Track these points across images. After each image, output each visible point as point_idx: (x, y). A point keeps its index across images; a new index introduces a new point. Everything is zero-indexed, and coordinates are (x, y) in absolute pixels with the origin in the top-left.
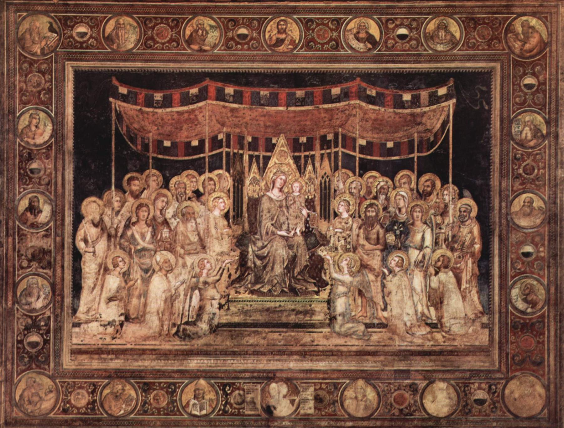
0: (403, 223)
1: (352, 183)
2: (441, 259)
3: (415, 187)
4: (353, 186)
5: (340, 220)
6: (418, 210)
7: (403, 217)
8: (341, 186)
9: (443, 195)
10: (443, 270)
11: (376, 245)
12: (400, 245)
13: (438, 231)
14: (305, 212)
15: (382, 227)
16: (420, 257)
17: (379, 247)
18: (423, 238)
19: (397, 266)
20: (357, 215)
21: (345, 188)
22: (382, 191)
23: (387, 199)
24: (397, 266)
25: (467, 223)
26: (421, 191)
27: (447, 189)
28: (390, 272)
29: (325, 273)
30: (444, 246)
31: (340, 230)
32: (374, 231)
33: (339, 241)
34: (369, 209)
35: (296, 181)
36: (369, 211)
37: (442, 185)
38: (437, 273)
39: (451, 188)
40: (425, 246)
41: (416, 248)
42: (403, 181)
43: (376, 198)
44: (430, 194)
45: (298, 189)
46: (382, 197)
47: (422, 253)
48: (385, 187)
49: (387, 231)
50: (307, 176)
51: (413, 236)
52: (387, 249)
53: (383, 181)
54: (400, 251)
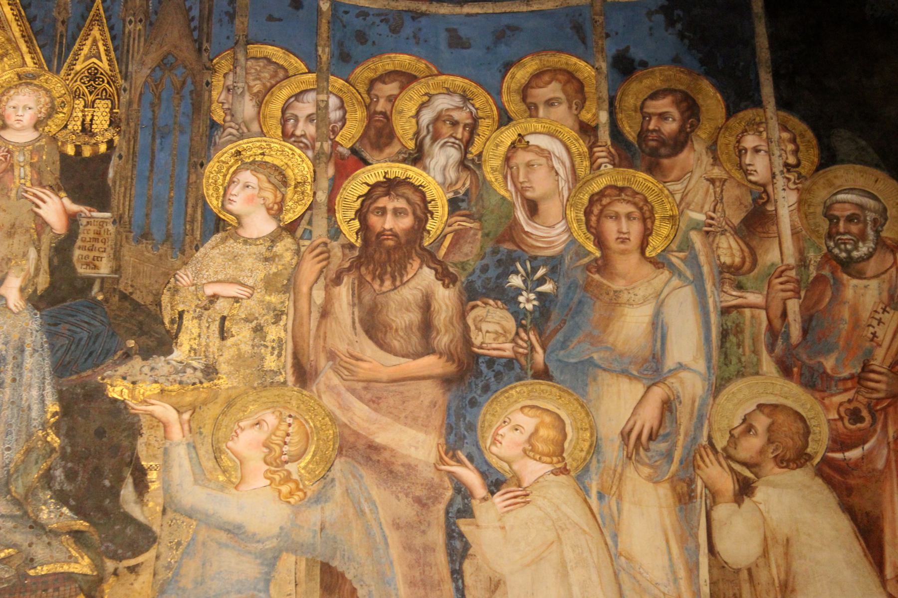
0: (555, 265)
1: (298, 96)
2: (761, 422)
3: (604, 117)
4: (306, 108)
5: (232, 246)
6: (623, 208)
7: (550, 233)
8: (247, 108)
9: (741, 152)
10: (775, 473)
11: (417, 356)
12: (539, 356)
13: (732, 298)
14: (54, 209)
15: (445, 276)
16: (649, 416)
17: (431, 364)
18: (658, 328)
19: (530, 450)
20: (320, 228)
21: (259, 115)
22: (446, 129)
23: (468, 164)
24: (530, 450)
25: (872, 267)
26: (630, 132)
27: (754, 126)
28: (495, 484)
29: (141, 486)
30: (768, 365)
31: (233, 290)
32: (410, 293)
33: (223, 334)
34: (383, 202)
35: (24, 79)
36: (383, 211)
37: (731, 111)
38: (745, 489)
39: (773, 124)
40: (670, 363)
41: (625, 373)
42: (542, 93)
43: (417, 157)
44: (679, 143)
45: (28, 118)
46: (443, 157)
47: (658, 393)
48: (456, 115)
49: (471, 295)
50: (78, 67)
51: (607, 322)
52: (472, 378)
53: (449, 92)
54: (543, 385)
